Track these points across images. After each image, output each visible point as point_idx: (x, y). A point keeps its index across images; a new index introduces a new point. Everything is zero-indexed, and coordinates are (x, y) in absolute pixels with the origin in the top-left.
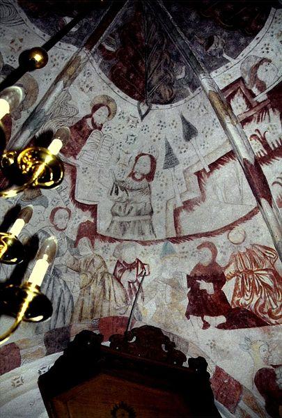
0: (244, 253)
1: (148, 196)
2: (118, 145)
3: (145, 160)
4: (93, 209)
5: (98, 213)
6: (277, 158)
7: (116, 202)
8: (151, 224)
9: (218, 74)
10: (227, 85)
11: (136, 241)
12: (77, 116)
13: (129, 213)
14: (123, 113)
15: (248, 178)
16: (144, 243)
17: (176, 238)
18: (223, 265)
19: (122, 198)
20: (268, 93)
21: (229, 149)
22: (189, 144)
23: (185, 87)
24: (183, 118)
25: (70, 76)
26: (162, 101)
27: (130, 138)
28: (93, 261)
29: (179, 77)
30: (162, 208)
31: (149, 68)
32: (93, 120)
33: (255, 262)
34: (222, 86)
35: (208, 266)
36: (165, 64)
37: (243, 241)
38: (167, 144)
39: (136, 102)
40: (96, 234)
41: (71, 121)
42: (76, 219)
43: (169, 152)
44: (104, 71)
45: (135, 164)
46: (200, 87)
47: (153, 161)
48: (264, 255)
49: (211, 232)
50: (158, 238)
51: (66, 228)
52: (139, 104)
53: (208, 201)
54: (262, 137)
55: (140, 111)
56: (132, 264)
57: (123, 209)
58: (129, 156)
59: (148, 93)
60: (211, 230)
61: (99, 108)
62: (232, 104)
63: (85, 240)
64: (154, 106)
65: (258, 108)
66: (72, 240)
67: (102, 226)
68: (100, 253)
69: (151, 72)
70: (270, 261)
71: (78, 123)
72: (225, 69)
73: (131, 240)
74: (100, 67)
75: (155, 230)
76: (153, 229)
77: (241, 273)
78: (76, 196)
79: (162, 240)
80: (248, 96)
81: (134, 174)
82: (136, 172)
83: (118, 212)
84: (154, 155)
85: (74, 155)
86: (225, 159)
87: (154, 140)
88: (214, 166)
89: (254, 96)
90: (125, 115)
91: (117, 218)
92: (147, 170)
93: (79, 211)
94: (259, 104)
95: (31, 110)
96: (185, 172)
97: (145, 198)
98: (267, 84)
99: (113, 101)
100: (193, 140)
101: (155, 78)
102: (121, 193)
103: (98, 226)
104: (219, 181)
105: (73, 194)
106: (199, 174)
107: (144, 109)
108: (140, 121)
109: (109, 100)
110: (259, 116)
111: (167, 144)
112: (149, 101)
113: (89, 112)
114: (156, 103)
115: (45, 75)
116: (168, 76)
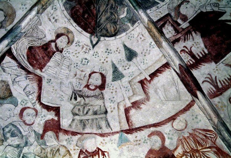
0: (188, 137)
1: (102, 101)
2: (75, 65)
3: (97, 76)
4: (57, 110)
5: (61, 113)
6: (203, 64)
8: (107, 120)
9: (152, 11)
10: (159, 18)
11: (95, 134)
12: (44, 39)
13: (87, 113)
15: (183, 80)
16: (102, 135)
17: (129, 130)
18: (172, 148)
19: (80, 102)
20: (189, 22)
21: (164, 61)
22: (131, 63)
23: (126, 23)
24: (125, 46)
25: (43, 6)
26: (108, 35)
27: (84, 61)
28: (58, 150)
29: (122, 16)
31: (99, 11)
32: (56, 45)
33: (199, 143)
34: (155, 20)
35: (160, 150)
36: (112, 7)
37: (186, 127)
41: (40, 41)
42: (42, 117)
43: (115, 69)
44: (66, 9)
46: (139, 21)
47: (103, 77)
48: (206, 136)
49: (158, 123)
50: (113, 131)
51: (32, 124)
52: (91, 37)
53: (152, 100)
54: (189, 51)
55: (91, 42)
56: (93, 152)
58: (84, 73)
59: (98, 29)
61: (61, 36)
62: (164, 30)
63: (50, 133)
64: (102, 38)
65: (183, 32)
66: (39, 134)
67: (65, 123)
68: (65, 143)
69: (100, 13)
70: (211, 141)
71: (44, 45)
72: (157, 8)
74: (64, 5)
75: (111, 125)
76: (108, 124)
77: (188, 152)
79: (117, 132)
80: (175, 25)
82: (90, 85)
83: (77, 112)
84: (103, 72)
85: (41, 69)
86: (163, 69)
87: (103, 63)
88: (153, 75)
89: (179, 25)
90: (80, 44)
91: (77, 117)
92: (99, 82)
93: (45, 111)
94: (183, 29)
95: (9, 28)
96: (130, 82)
97: (99, 102)
98: (188, 16)
99: (72, 32)
100: (134, 60)
101: (103, 18)
102: (79, 99)
103: (61, 123)
104: (159, 85)
105: (39, 98)
106: (142, 82)
107: (95, 40)
108: (91, 48)
109: (69, 32)
110: (185, 37)
112: (99, 34)
113: (54, 38)
115: (22, 5)
116: (113, 16)
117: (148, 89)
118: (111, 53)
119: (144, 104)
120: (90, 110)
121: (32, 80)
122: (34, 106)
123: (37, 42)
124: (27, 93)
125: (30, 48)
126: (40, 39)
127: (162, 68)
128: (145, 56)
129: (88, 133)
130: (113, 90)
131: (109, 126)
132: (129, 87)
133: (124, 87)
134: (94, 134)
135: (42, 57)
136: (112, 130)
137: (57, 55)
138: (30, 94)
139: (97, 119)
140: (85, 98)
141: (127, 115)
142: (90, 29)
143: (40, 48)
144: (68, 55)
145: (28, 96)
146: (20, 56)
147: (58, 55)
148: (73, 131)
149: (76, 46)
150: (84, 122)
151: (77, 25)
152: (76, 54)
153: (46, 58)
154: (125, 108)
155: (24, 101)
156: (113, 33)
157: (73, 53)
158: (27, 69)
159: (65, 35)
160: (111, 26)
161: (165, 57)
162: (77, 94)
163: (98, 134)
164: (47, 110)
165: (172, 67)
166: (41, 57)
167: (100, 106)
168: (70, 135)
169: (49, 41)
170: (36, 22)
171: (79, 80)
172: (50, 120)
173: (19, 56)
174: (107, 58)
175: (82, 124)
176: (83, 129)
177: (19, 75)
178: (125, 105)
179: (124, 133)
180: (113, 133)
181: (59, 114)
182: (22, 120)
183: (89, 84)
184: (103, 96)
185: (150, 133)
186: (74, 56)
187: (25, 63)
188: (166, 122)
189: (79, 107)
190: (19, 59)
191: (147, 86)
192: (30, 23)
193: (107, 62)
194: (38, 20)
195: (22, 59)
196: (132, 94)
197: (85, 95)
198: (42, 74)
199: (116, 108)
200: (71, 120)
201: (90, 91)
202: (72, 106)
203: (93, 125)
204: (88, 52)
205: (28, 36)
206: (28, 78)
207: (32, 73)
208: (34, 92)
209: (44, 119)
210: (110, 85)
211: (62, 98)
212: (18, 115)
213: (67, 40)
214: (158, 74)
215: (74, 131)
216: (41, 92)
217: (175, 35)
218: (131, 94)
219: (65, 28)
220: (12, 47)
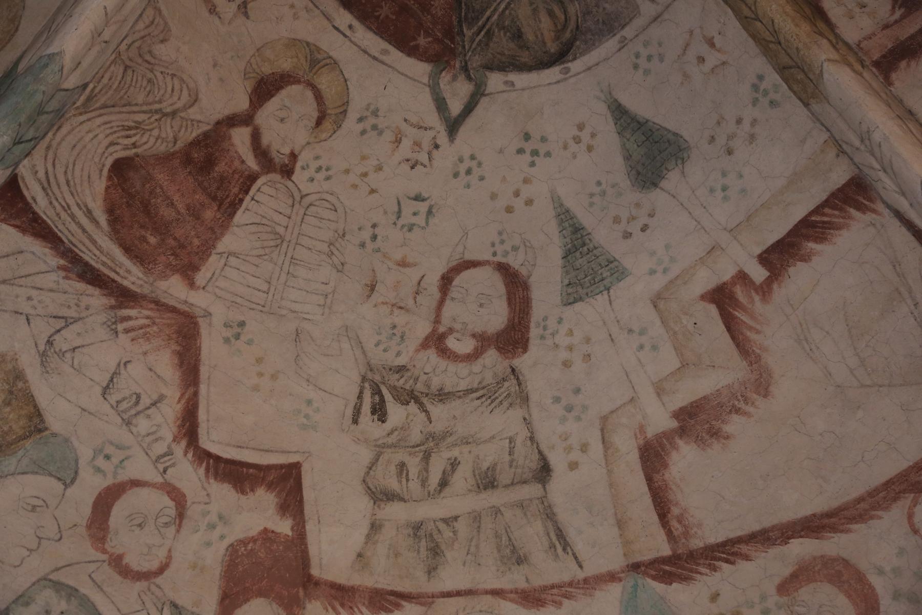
1: (517, 414)
2: (366, 235)
5: (308, 494)
7: (380, 449)
8: (549, 515)
11: (497, 593)
12: (193, 113)
14: (375, 113)
21: (839, 176)
22: (657, 197)
24: (619, 112)
26: (525, 57)
27: (409, 207)
30: (584, 448)
32: (256, 137)
38: (564, 216)
39: (421, 69)
40: (309, 583)
41: (168, 131)
42: (211, 527)
45: (441, 302)
49: (829, 515)
50: (590, 570)
51: (161, 570)
55: (441, 105)
57: (413, 471)
58: (413, 275)
59: (468, 33)
60: (835, 504)
61: (279, 88)
64: (495, 81)
71: (195, 143)
73: (470, 593)
75: (571, 534)
76: (561, 535)
78: (202, 431)
79: (612, 577)
81: (442, 338)
82: (451, 330)
83: (393, 484)
84: (515, 261)
85: (188, 271)
87: (509, 210)
90: (381, 122)
91: (395, 512)
96: (656, 301)
99: (334, 64)
100: (672, 180)
102: (396, 413)
103: (313, 550)
108: (443, 139)
111: (564, 216)
113: (242, 103)
114: (502, 68)
117: (758, 332)
118: (548, 154)
119: (745, 414)
120: (460, 468)
121: (147, 337)
122: (165, 471)
123: (156, 132)
124: (124, 405)
125: (120, 168)
126: (165, 115)
127: (827, 210)
128: (730, 152)
129: (458, 594)
130: (570, 348)
131: (566, 546)
132: (657, 330)
133: (630, 331)
134: (487, 592)
135: (188, 208)
136: (581, 567)
137: (264, 189)
138: (138, 413)
139: (496, 511)
140: (429, 407)
141: (656, 477)
142: (427, 34)
143: (176, 162)
144: (326, 186)
145: (128, 423)
146: (73, 217)
147: (272, 191)
148: (377, 586)
149: (363, 132)
150: (431, 535)
151: (356, 23)
152: (365, 175)
153: (209, 214)
154: (642, 442)
155: (110, 450)
156: (553, 47)
157: (347, 171)
158: (113, 281)
159: (298, 81)
160: (535, 11)
161: (841, 152)
162: (385, 391)
163: (511, 592)
164: (235, 487)
165: (884, 202)
166: (181, 207)
167: (511, 440)
168: (364, 610)
169: (218, 123)
170: (141, 25)
171: (392, 313)
172: (253, 540)
173: (64, 215)
174: (526, 181)
175: (423, 543)
176: (429, 572)
177: (72, 313)
178: (642, 429)
179: (649, 581)
180: (590, 584)
181: (301, 501)
182: (104, 551)
183: (442, 329)
184: (519, 384)
185: (787, 572)
186: (355, 186)
187: (99, 248)
188: (876, 507)
189: (400, 456)
190: (65, 228)
191: (753, 317)
192: (106, 36)
193: (529, 202)
194: (150, 12)
195: (84, 231)
196: (674, 363)
197: (429, 387)
198: (198, 300)
199: (596, 448)
200: (365, 530)
201: (452, 367)
202: (365, 455)
203: (477, 546)
204: (426, 161)
205: (104, 106)
206: (120, 327)
207: (144, 297)
208: (161, 398)
209: (222, 537)
210: (552, 323)
211: (307, 416)
212: (82, 530)
213: (310, 109)
214: (811, 245)
215: (384, 582)
216: (196, 394)
217: (896, 22)
218: (669, 360)
219: (293, 43)
220: (24, 170)
